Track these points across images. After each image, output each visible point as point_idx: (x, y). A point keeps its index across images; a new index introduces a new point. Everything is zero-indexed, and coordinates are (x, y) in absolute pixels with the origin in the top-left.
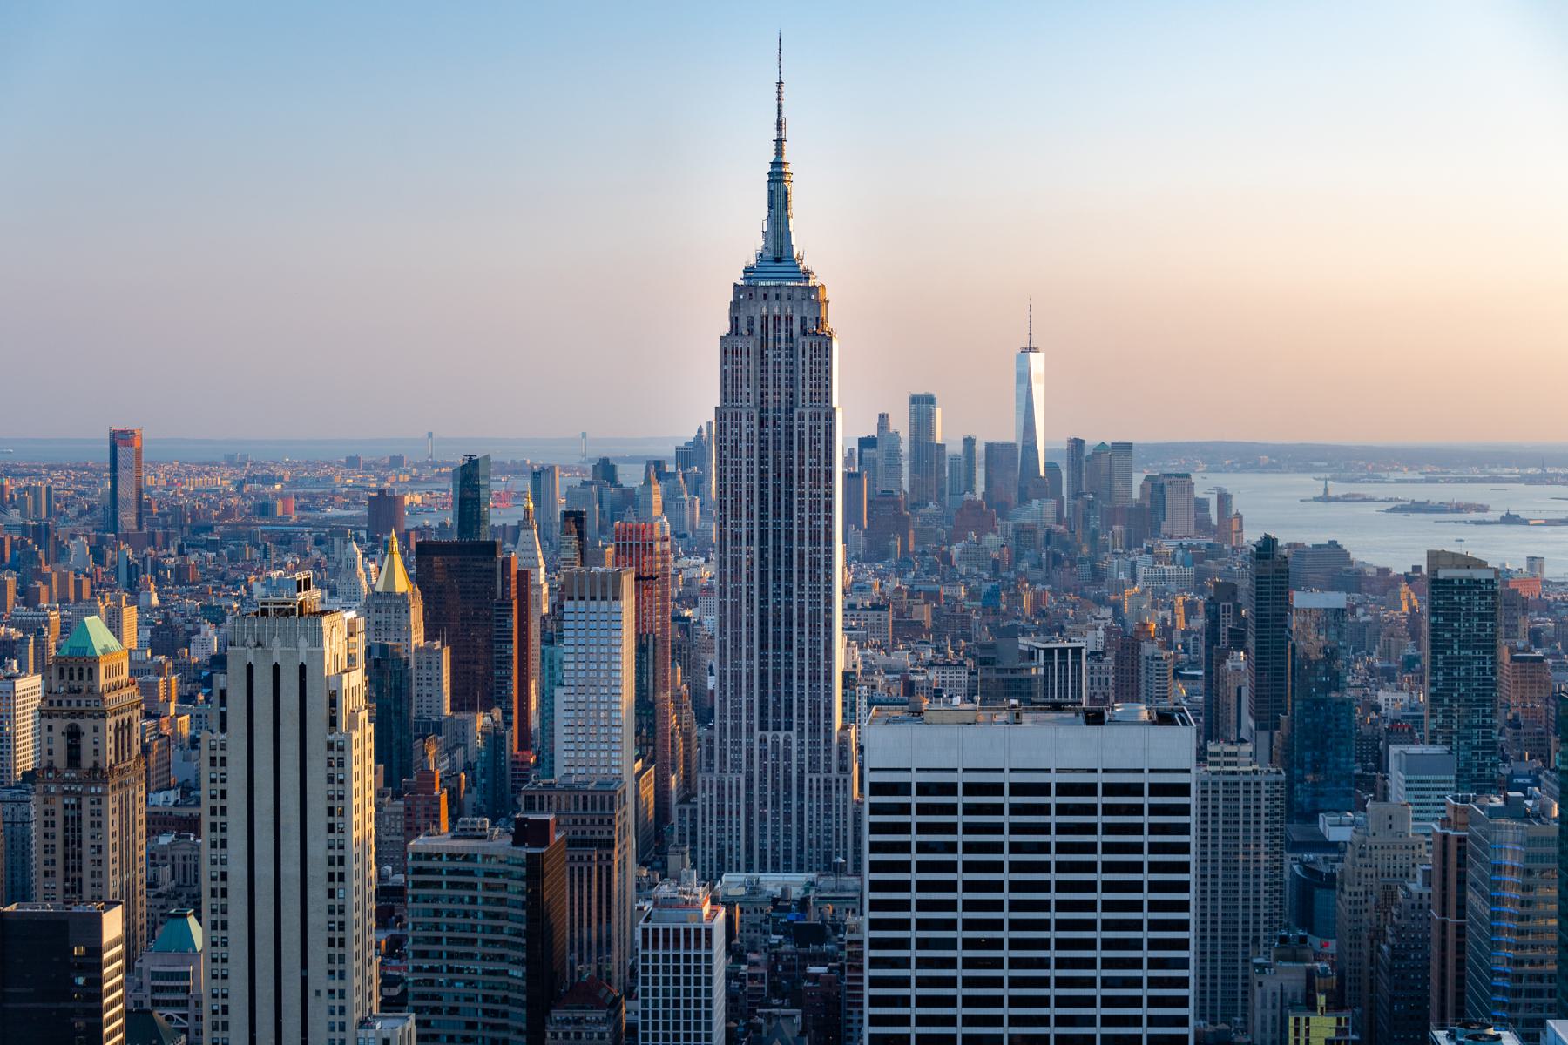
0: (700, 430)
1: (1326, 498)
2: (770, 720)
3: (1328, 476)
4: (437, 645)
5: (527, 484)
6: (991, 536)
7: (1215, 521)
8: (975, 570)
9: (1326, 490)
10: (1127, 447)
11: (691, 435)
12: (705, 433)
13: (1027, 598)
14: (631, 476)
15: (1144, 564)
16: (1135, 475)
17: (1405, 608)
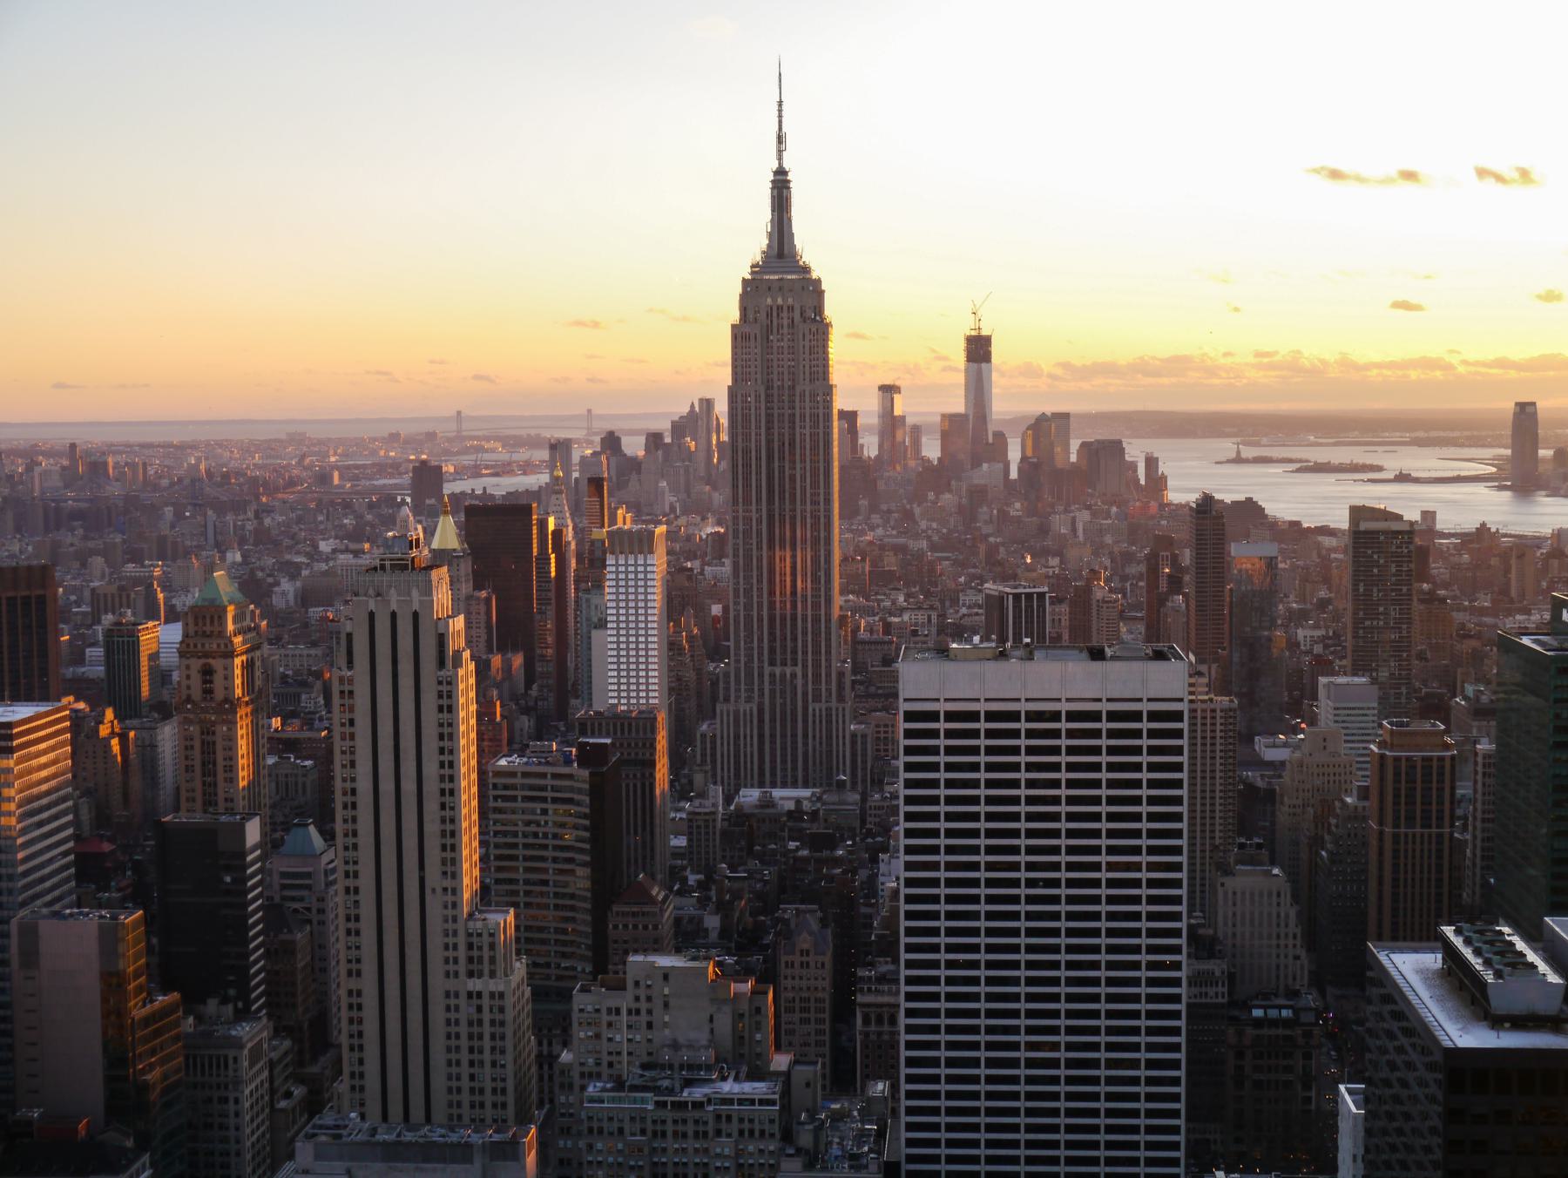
0: (692, 406)
1: (1238, 460)
2: (778, 657)
3: (1239, 440)
4: (484, 594)
5: (544, 454)
6: (947, 496)
7: (1143, 482)
8: (934, 525)
9: (1238, 452)
10: (1064, 417)
11: (686, 409)
12: (697, 409)
13: (982, 548)
14: (634, 446)
15: (1083, 516)
16: (1072, 441)
17: (1314, 555)
